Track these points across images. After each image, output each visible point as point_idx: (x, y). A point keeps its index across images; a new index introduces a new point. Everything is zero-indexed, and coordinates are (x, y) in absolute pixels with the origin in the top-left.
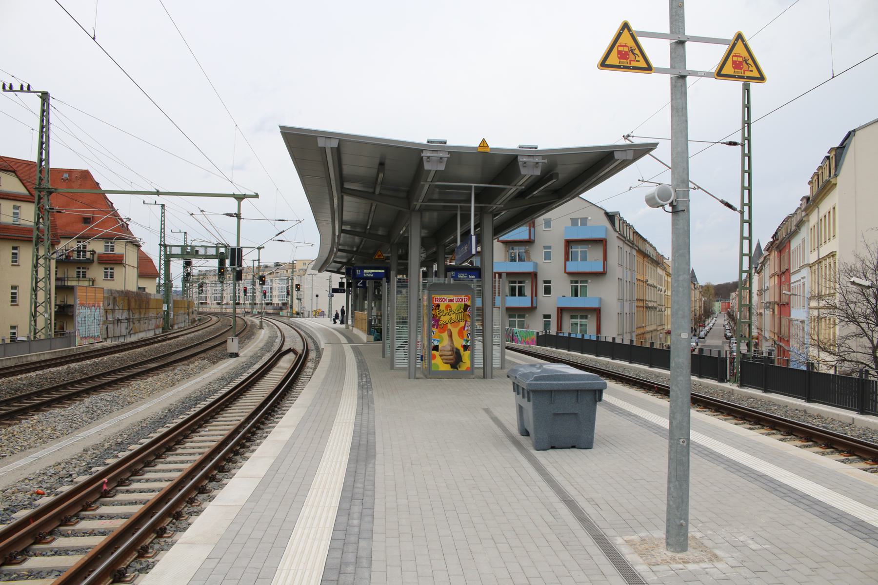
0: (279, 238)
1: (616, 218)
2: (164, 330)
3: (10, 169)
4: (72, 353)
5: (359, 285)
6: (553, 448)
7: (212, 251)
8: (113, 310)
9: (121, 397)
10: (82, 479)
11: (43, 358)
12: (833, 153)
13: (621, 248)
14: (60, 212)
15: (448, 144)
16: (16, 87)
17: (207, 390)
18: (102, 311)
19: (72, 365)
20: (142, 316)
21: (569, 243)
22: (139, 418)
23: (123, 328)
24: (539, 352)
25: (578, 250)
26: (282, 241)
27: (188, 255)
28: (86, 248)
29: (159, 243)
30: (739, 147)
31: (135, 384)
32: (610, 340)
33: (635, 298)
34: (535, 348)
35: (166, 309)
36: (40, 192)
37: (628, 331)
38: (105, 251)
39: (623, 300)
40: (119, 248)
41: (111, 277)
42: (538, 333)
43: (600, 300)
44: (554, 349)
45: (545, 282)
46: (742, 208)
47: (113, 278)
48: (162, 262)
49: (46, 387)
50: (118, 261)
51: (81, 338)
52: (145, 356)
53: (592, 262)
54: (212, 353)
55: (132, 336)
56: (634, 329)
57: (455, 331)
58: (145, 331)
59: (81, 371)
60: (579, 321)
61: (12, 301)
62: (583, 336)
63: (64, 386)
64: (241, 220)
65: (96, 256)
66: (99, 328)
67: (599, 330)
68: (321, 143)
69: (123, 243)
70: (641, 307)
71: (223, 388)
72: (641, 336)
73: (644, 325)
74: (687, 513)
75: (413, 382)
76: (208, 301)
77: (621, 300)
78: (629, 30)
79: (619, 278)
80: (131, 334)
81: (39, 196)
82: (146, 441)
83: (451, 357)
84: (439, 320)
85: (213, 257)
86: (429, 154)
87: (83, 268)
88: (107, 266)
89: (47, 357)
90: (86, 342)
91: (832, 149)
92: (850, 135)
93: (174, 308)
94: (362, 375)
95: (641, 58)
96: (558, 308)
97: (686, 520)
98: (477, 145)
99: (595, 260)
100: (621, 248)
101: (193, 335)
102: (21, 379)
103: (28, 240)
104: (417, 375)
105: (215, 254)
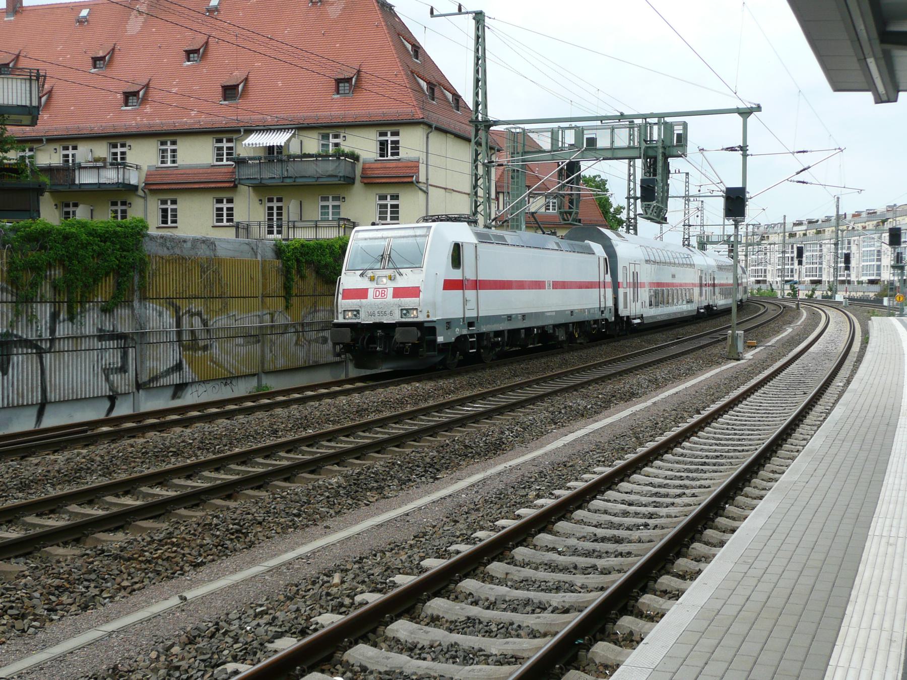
47: (397, 218)
87: (335, 199)
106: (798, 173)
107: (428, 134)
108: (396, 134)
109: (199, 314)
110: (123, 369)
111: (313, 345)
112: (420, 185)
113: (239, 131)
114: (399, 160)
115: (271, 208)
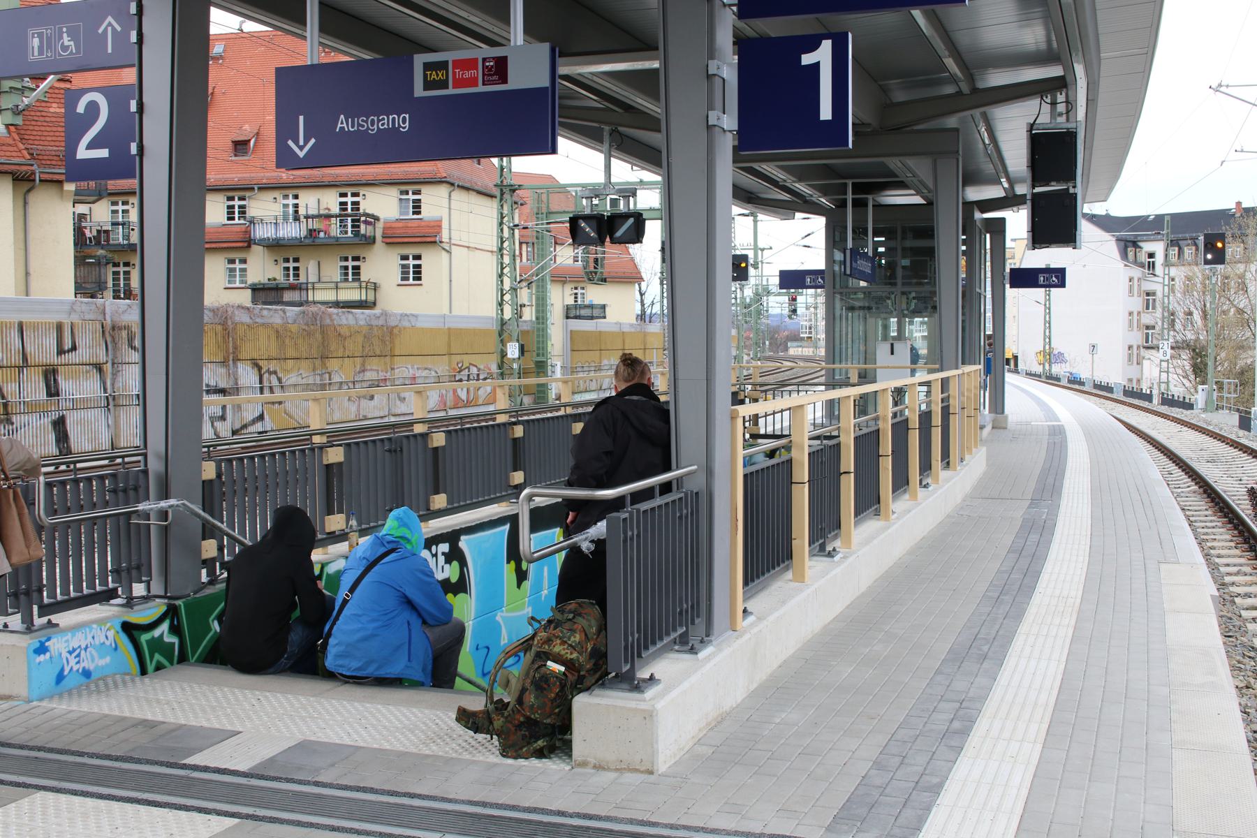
5: (83, 153)
28: (358, 209)
35: (516, 355)
38: (401, 214)
41: (414, 279)
50: (429, 237)
65: (380, 225)
69: (443, 191)
87: (356, 259)
106: (803, 238)
107: (450, 193)
108: (417, 192)
109: (275, 373)
110: (223, 418)
111: (362, 400)
112: (443, 245)
113: (253, 189)
114: (421, 219)
115: (287, 269)
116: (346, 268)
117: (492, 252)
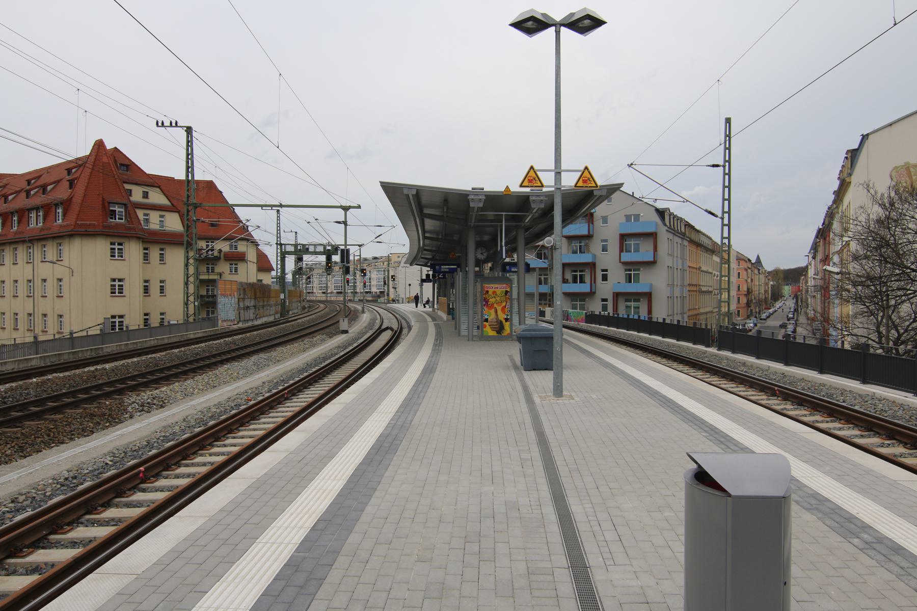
0: (378, 240)
1: (666, 213)
2: (282, 315)
3: (157, 185)
4: (217, 332)
6: (534, 370)
7: (321, 249)
8: (244, 299)
9: (273, 357)
10: (268, 395)
11: (197, 336)
12: (850, 154)
13: (671, 240)
14: (204, 222)
15: (485, 190)
16: (167, 123)
17: (330, 353)
18: (237, 300)
19: (227, 339)
20: (265, 303)
21: (623, 237)
22: (289, 369)
23: (251, 314)
24: (583, 328)
25: (632, 242)
26: (380, 242)
27: (300, 251)
29: (276, 242)
30: (721, 168)
31: (279, 349)
32: (661, 320)
33: (687, 282)
34: (584, 325)
35: (283, 298)
36: (188, 206)
37: (679, 312)
38: (230, 249)
39: (674, 285)
40: (242, 247)
42: (586, 313)
43: (651, 285)
44: (598, 326)
45: (603, 270)
46: (723, 215)
47: (237, 272)
48: (279, 258)
49: (214, 353)
50: (241, 258)
51: (222, 321)
52: (276, 333)
53: (644, 253)
54: (328, 330)
55: (258, 319)
56: (686, 310)
57: (499, 309)
58: (267, 316)
59: (234, 342)
60: (632, 304)
61: (161, 293)
62: (628, 315)
63: (224, 353)
64: (348, 226)
65: (222, 254)
66: (234, 313)
67: (650, 312)
68: (406, 192)
69: (245, 243)
70: (694, 291)
71: (341, 352)
72: (695, 317)
73: (697, 307)
74: (562, 381)
75: (471, 342)
76: (315, 291)
77: (671, 286)
78: (533, 169)
79: (668, 267)
80: (257, 318)
81: (188, 209)
82: (297, 379)
83: (497, 326)
84: (488, 301)
85: (320, 253)
86: (473, 197)
87: (212, 264)
88: (232, 262)
89: (200, 335)
90: (225, 324)
91: (848, 152)
92: (865, 138)
93: (289, 296)
94: (437, 340)
95: (538, 182)
96: (614, 293)
97: (562, 384)
98: (503, 190)
99: (647, 251)
100: (671, 240)
101: (308, 318)
102: (195, 348)
103: (180, 244)
104: (474, 339)
105: (323, 251)
116: (208, 267)
117: (254, 262)
